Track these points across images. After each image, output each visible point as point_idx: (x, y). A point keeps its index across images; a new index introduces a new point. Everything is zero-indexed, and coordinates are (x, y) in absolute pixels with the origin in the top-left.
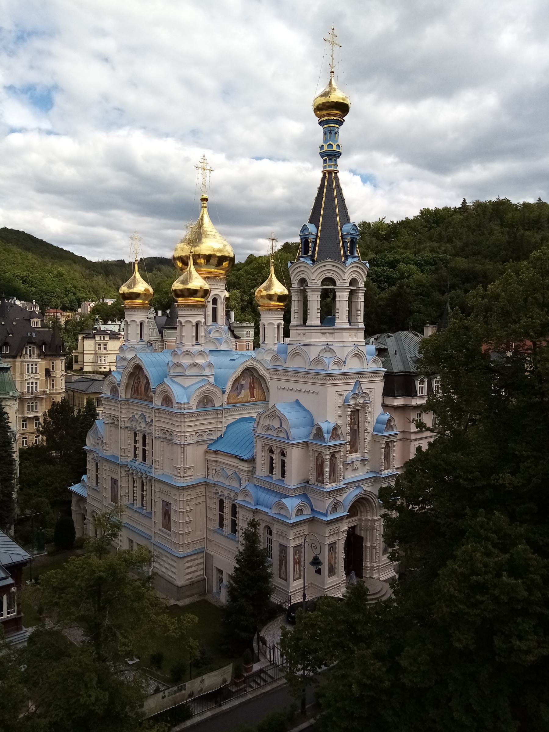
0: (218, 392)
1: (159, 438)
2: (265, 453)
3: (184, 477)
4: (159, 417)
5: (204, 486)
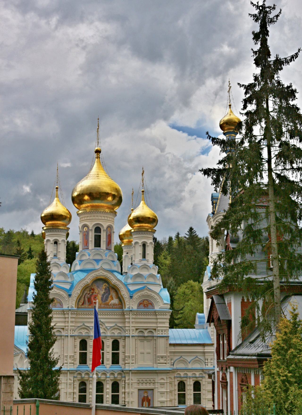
4: (135, 318)
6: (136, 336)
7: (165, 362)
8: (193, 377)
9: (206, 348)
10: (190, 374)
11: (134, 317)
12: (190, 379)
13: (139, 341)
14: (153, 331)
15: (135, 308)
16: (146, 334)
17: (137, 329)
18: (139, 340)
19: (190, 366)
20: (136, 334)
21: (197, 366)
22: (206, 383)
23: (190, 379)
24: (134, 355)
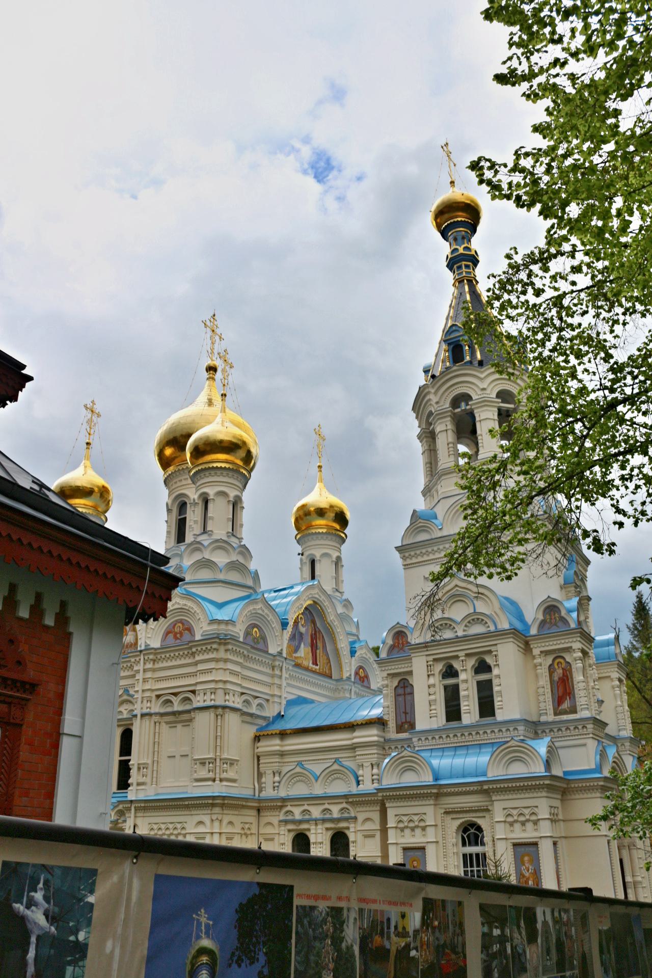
0: (277, 625)
1: (150, 715)
2: (436, 680)
3: (221, 780)
4: (154, 670)
5: (254, 813)
6: (156, 714)
7: (211, 775)
8: (324, 821)
9: (356, 734)
10: (316, 812)
11: (149, 666)
12: (316, 824)
13: (164, 727)
14: (190, 695)
15: (156, 644)
16: (177, 707)
17: (158, 697)
18: (167, 723)
19: (318, 790)
20: (156, 708)
21: (338, 788)
22: (359, 835)
23: (316, 824)
24: (149, 762)
